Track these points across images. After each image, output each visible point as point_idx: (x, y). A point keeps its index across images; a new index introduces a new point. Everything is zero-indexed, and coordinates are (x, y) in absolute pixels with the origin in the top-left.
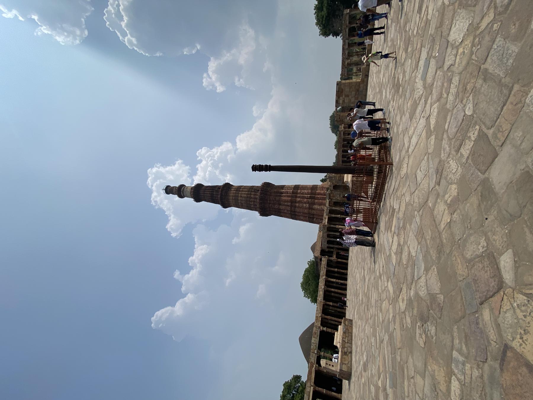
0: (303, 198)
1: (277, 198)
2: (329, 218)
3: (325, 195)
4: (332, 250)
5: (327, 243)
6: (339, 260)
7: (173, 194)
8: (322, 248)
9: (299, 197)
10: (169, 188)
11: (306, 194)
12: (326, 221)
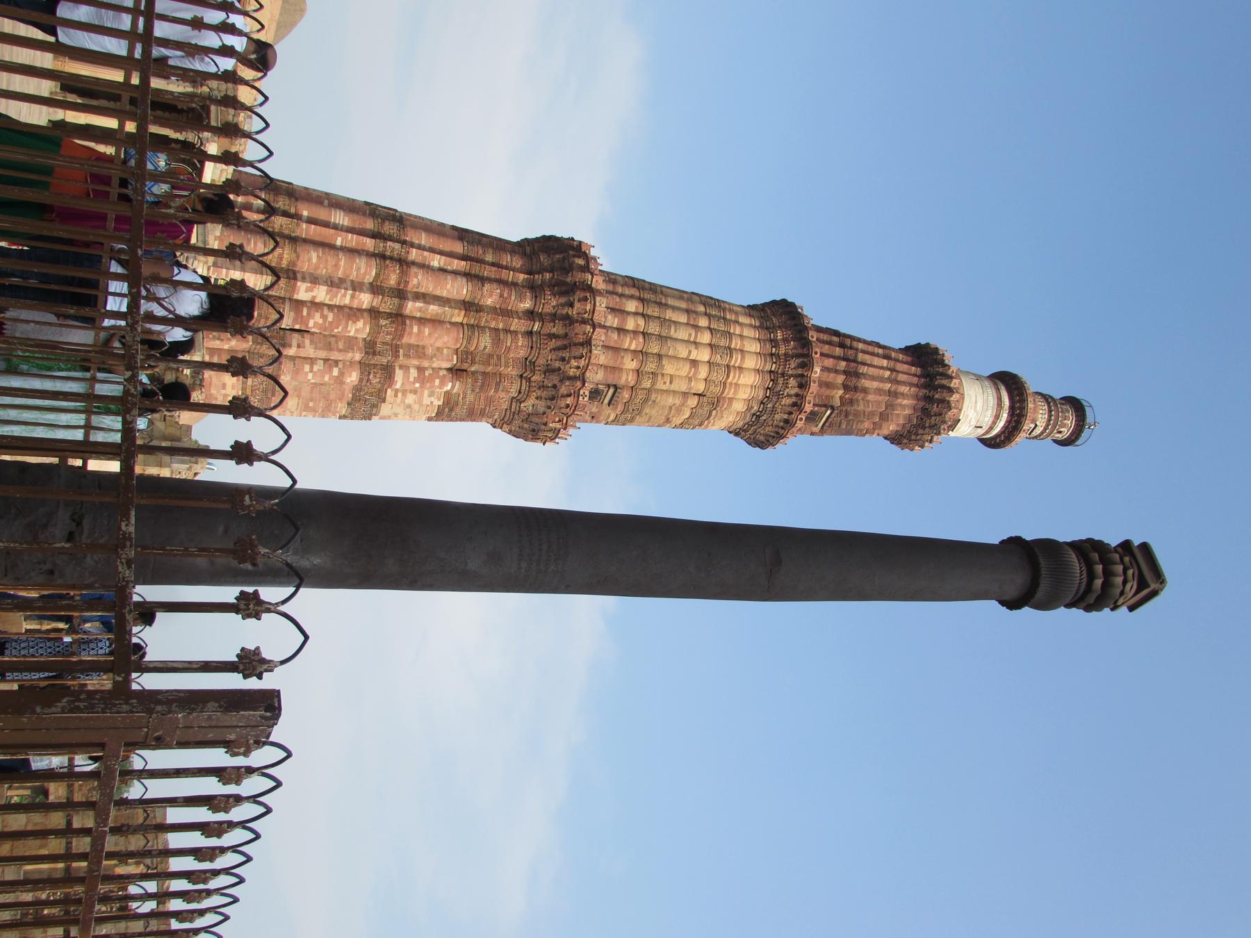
0: (327, 340)
7: (1047, 398)
9: (351, 343)
10: (1066, 432)
11: (312, 361)
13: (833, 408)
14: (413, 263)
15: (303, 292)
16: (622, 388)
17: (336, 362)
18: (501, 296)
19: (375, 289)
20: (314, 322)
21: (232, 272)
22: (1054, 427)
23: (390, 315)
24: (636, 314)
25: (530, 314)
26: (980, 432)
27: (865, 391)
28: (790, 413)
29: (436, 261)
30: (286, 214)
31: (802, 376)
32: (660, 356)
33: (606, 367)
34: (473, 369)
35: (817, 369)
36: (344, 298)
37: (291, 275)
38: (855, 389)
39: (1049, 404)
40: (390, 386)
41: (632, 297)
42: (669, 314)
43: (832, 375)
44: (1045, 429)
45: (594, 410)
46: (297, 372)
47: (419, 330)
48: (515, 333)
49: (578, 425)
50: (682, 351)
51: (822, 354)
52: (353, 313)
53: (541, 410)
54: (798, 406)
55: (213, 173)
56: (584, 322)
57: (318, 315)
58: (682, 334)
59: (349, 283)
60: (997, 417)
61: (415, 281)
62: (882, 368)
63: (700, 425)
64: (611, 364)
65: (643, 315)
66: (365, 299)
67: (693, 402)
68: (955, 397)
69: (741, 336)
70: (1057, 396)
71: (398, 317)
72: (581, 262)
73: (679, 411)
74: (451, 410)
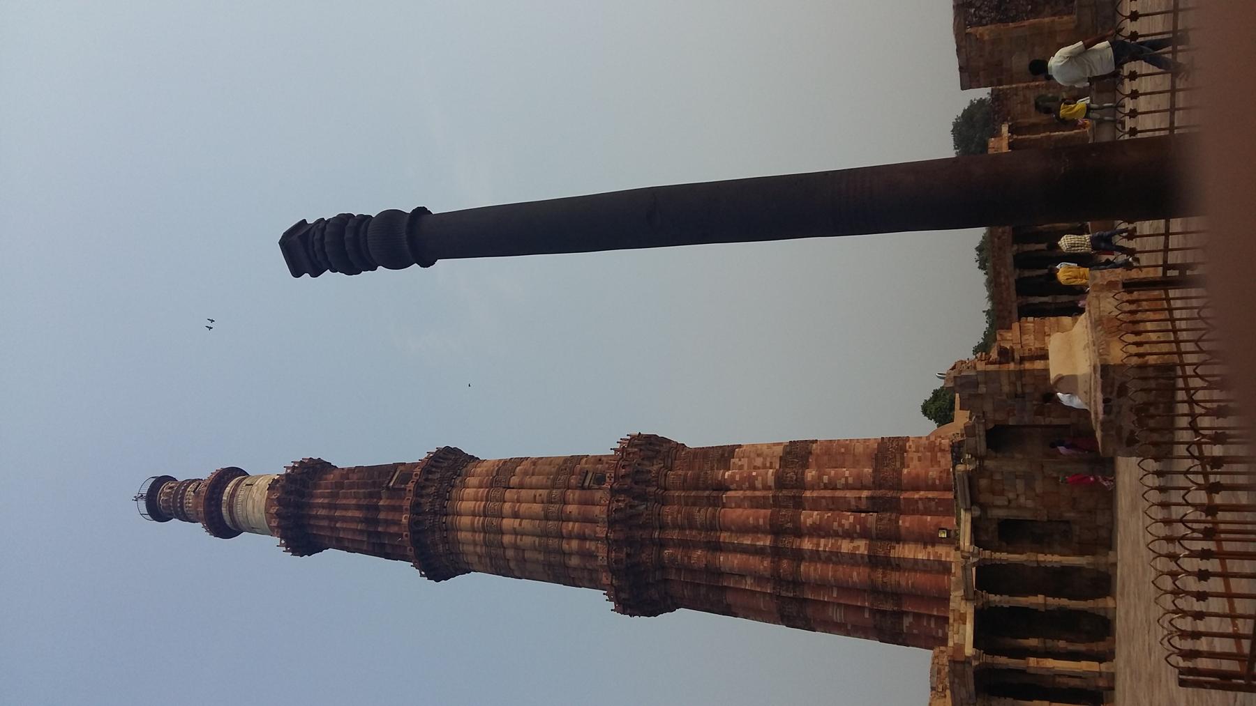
0: (836, 505)
1: (701, 515)
2: (978, 613)
7: (185, 517)
9: (815, 505)
10: (165, 488)
11: (847, 487)
12: (964, 635)
14: (768, 580)
15: (862, 547)
16: (576, 488)
17: (826, 487)
18: (690, 558)
19: (798, 555)
20: (849, 519)
22: (177, 492)
24: (571, 554)
25: (662, 544)
26: (248, 481)
27: (358, 507)
28: (426, 480)
30: (883, 613)
32: (547, 518)
33: (593, 504)
34: (707, 493)
36: (825, 544)
41: (575, 569)
42: (541, 557)
43: (390, 518)
44: (185, 490)
46: (859, 477)
47: (757, 519)
48: (674, 528)
49: (613, 452)
51: (401, 536)
52: (818, 531)
53: (646, 462)
54: (420, 487)
55: (965, 630)
56: (615, 541)
57: (847, 527)
58: (528, 540)
59: (823, 557)
60: (233, 495)
61: (765, 563)
62: (344, 529)
63: (505, 462)
64: (589, 507)
65: (564, 554)
66: (807, 545)
67: (514, 480)
68: (273, 510)
70: (175, 521)
71: (776, 530)
72: (623, 596)
73: (525, 473)
74: (723, 455)
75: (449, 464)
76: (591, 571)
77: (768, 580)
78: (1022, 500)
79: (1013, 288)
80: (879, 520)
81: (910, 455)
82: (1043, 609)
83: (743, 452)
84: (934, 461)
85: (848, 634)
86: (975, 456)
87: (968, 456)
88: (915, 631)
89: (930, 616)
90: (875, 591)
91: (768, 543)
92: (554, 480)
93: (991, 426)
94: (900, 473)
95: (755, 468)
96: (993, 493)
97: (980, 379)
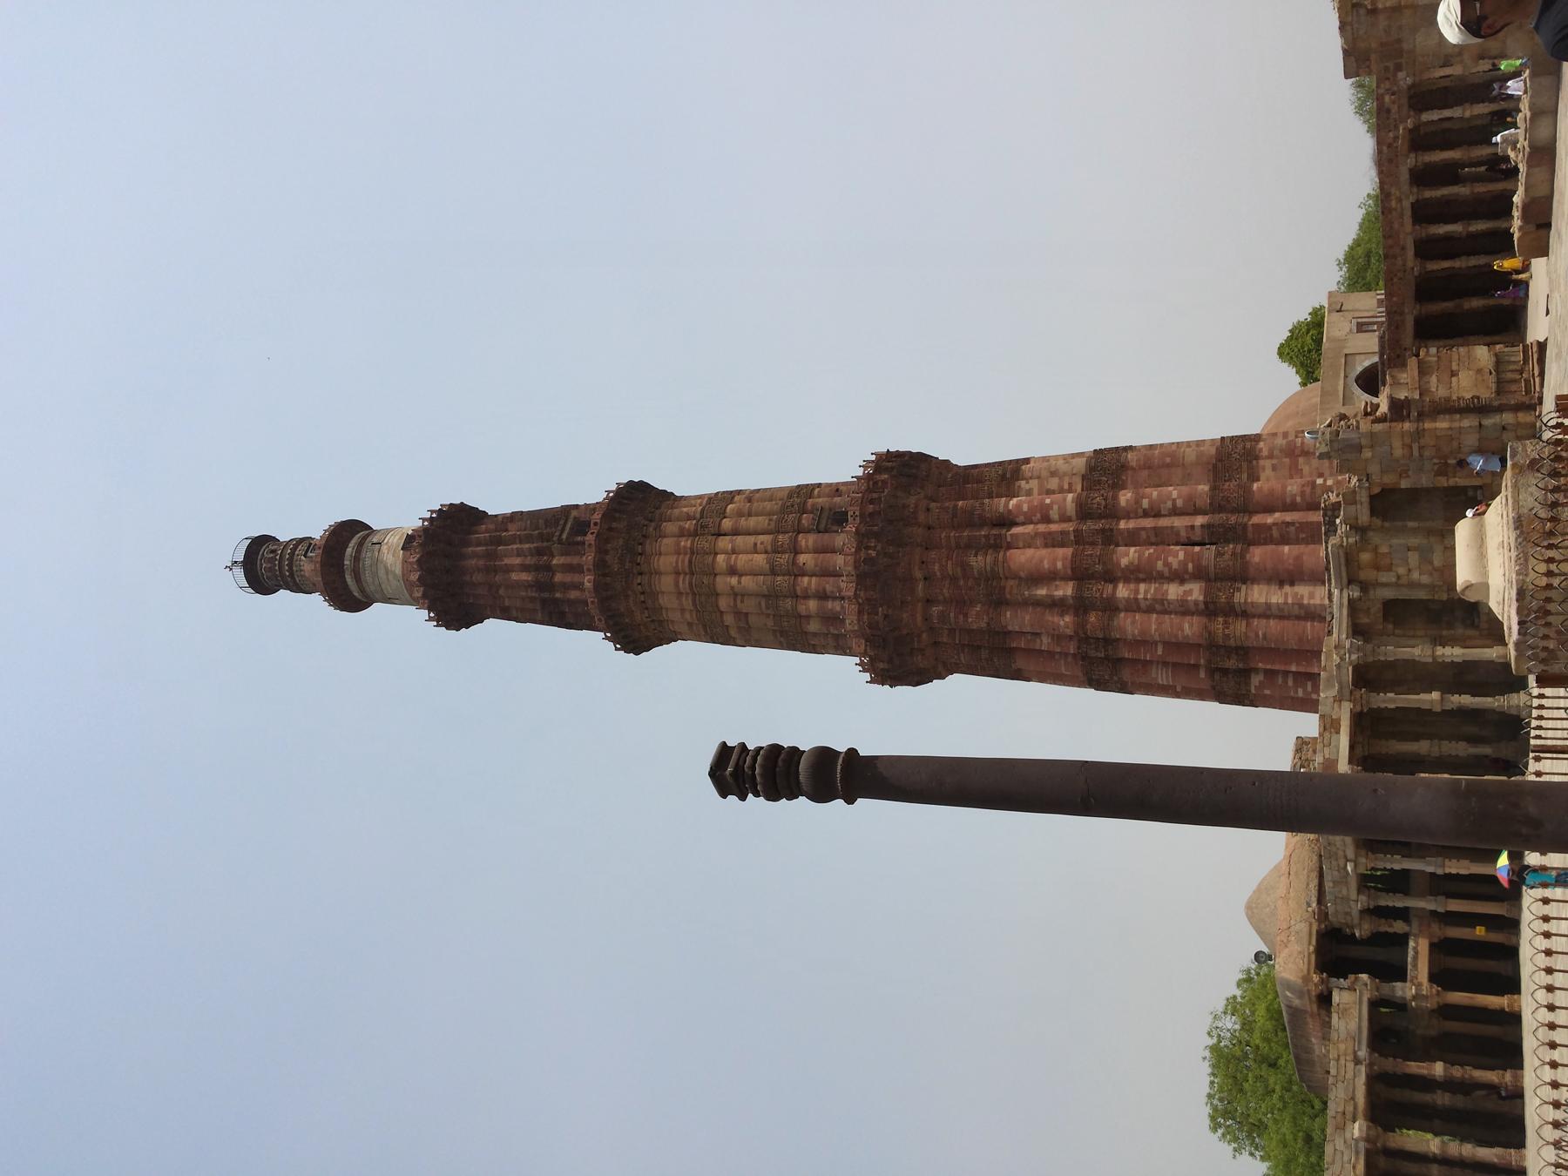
1: (978, 562)
2: (1358, 720)
3: (1313, 506)
4: (1399, 927)
5: (1359, 892)
6: (1459, 997)
7: (297, 588)
8: (1322, 915)
9: (1132, 539)
10: (264, 551)
11: (1175, 512)
13: (560, 541)
15: (1195, 592)
17: (1146, 514)
18: (966, 615)
21: (1281, 601)
23: (1092, 576)
24: (808, 617)
25: (929, 602)
27: (525, 568)
29: (1045, 643)
30: (1225, 672)
31: (605, 575)
35: (588, 585)
37: (1211, 607)
38: (537, 568)
39: (296, 584)
40: (1079, 496)
41: (815, 634)
45: (837, 499)
46: (1190, 499)
47: (1054, 562)
50: (747, 581)
52: (1136, 574)
57: (1175, 565)
59: (1143, 605)
60: (357, 558)
67: (727, 524)
68: (414, 577)
69: (683, 610)
70: (283, 594)
71: (1079, 574)
72: (881, 665)
73: (740, 514)
74: (1003, 477)
75: (637, 503)
76: (837, 637)
77: (1071, 637)
78: (1415, 575)
79: (1408, 213)
80: (1219, 554)
81: (1262, 462)
82: (1438, 709)
83: (1031, 470)
84: (1295, 471)
85: (1177, 695)
86: (1355, 528)
87: (1342, 529)
88: (1267, 692)
89: (1286, 673)
90: (1213, 647)
91: (1069, 592)
92: (779, 521)
93: (1377, 490)
94: (1247, 490)
95: (1049, 492)
96: (1378, 568)
97: (1364, 442)
